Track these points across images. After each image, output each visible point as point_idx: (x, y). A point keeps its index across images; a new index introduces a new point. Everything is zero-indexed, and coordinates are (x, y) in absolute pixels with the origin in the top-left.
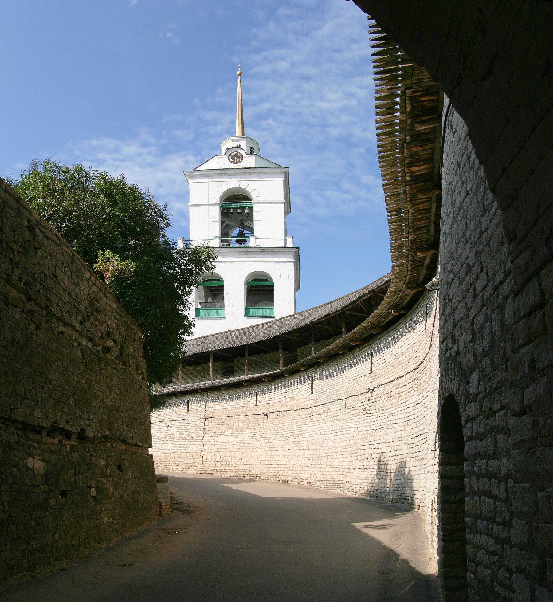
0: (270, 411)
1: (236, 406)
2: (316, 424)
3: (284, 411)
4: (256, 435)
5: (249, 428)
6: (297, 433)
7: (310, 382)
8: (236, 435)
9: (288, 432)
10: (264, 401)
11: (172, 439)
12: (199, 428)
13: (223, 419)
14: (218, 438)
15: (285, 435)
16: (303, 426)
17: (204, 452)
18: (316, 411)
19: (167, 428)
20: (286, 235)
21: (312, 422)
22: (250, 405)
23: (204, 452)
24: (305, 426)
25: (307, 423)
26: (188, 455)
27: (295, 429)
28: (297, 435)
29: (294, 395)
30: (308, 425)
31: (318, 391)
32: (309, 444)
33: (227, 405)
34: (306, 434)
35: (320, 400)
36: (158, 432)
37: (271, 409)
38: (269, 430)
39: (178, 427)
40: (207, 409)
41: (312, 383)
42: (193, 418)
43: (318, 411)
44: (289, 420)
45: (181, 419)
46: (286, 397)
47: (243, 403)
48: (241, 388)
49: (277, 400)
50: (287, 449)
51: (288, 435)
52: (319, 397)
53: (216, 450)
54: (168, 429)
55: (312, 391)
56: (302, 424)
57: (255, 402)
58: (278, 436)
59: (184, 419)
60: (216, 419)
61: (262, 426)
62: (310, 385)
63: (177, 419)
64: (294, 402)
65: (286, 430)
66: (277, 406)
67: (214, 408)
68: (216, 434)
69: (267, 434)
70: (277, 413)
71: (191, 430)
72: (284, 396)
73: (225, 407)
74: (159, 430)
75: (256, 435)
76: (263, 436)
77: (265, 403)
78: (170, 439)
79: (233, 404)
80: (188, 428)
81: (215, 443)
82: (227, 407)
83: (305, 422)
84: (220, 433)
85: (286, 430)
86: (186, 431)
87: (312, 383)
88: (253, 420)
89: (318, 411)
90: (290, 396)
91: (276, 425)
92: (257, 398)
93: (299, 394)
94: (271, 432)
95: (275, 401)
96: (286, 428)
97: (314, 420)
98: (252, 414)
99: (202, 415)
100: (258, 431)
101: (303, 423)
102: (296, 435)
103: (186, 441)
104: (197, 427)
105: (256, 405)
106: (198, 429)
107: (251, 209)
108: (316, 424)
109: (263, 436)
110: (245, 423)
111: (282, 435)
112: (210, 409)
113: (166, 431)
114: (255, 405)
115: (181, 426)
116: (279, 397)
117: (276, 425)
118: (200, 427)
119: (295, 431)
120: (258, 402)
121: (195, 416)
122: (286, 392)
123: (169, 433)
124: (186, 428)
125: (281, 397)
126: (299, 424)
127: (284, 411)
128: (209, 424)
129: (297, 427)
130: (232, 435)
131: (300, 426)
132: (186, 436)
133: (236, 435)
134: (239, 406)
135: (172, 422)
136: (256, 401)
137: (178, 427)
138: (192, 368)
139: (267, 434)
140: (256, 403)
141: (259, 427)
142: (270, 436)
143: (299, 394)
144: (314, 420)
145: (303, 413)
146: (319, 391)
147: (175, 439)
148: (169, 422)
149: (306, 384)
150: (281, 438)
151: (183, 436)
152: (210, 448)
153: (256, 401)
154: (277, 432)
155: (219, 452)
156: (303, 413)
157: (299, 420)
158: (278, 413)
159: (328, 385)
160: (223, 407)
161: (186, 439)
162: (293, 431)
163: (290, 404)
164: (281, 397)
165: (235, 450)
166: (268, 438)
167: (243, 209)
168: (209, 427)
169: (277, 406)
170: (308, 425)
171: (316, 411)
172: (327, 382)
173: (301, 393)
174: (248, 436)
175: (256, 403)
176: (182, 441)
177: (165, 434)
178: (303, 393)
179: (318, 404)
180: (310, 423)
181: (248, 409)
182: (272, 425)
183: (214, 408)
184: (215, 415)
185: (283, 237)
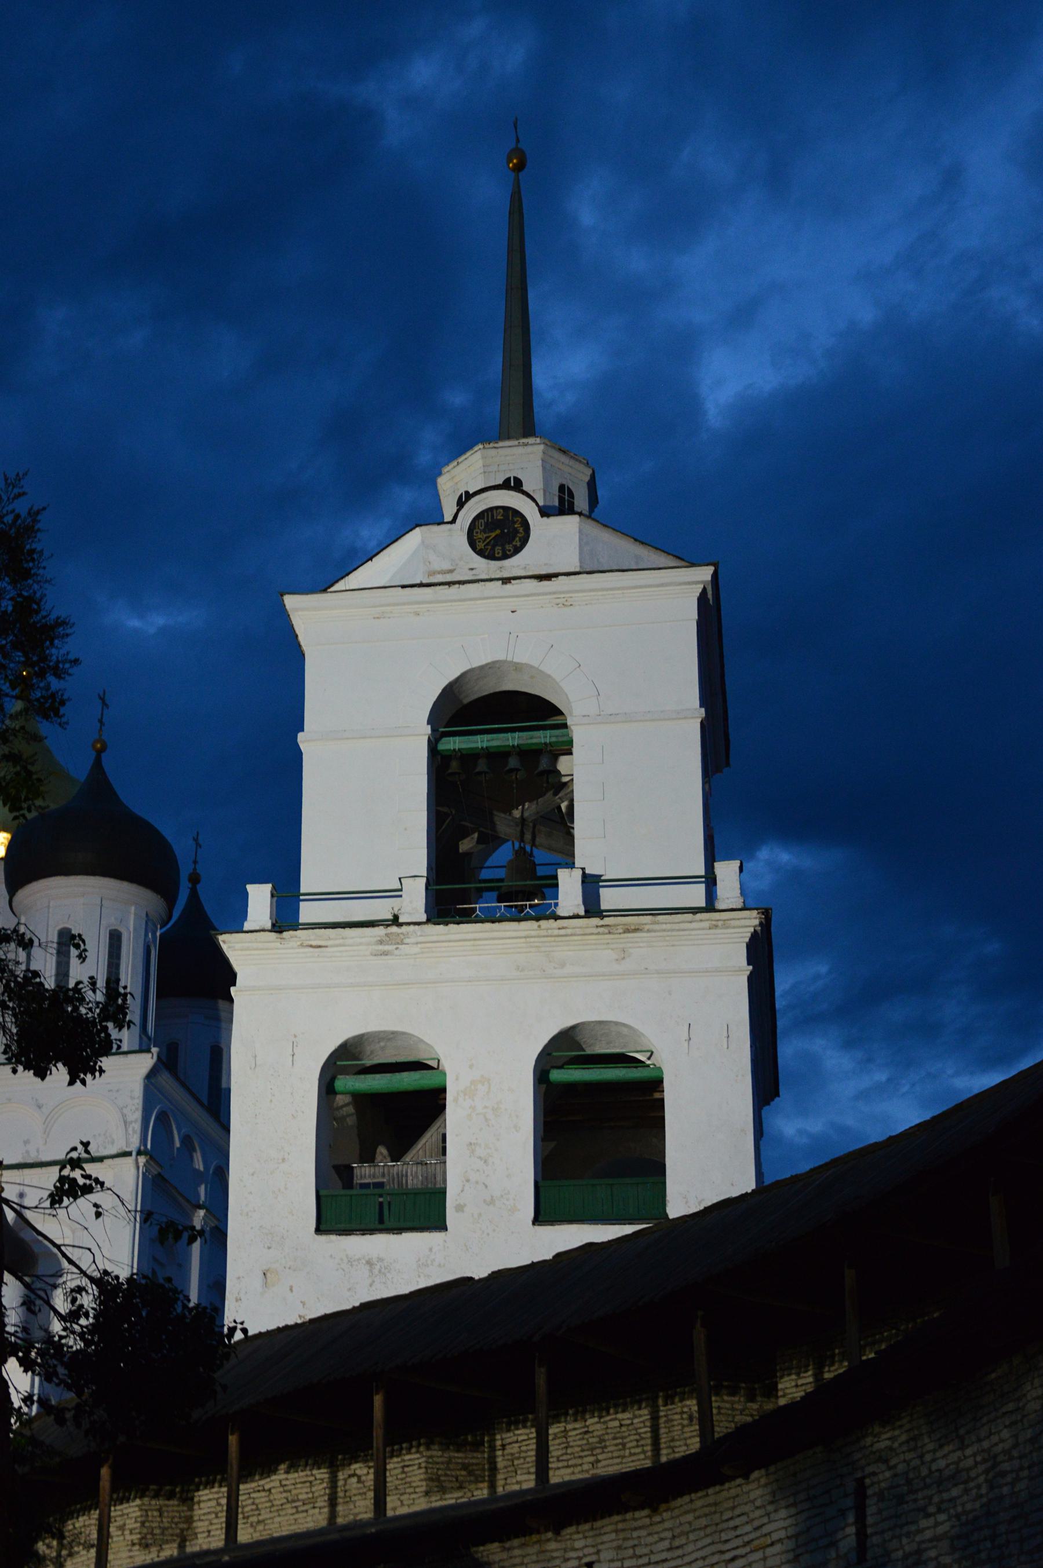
7: (850, 1502)
48: (516, 1542)
122: (728, 1556)
159: (940, 1510)
172: (936, 1499)
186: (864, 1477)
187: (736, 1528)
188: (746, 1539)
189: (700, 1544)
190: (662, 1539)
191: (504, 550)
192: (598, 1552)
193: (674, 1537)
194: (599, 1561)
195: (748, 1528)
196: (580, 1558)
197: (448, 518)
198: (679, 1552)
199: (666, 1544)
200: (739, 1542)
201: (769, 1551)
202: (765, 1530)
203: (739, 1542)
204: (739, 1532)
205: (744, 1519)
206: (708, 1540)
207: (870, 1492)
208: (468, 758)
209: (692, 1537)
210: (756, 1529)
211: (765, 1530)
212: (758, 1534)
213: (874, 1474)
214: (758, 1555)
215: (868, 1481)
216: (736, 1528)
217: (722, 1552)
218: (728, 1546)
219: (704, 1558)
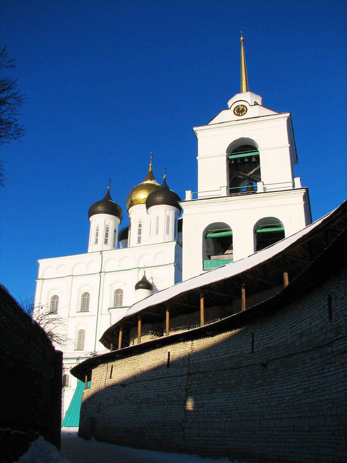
0: (271, 358)
1: (227, 356)
2: (341, 370)
3: (290, 355)
4: (254, 396)
5: (243, 385)
6: (311, 389)
7: (327, 302)
8: (226, 396)
9: (298, 388)
10: (262, 344)
11: (149, 405)
12: (180, 389)
13: (210, 376)
14: (205, 402)
15: (293, 394)
16: (319, 376)
17: (186, 421)
18: (339, 347)
19: (144, 390)
20: (293, 177)
21: (334, 368)
22: (245, 352)
23: (186, 421)
24: (323, 375)
25: (325, 371)
26: (166, 427)
27: (308, 383)
28: (312, 393)
29: (303, 329)
30: (328, 374)
31: (339, 314)
32: (330, 405)
33: (215, 355)
34: (326, 389)
35: (344, 328)
36: (134, 395)
37: (273, 355)
38: (271, 387)
39: (156, 388)
40: (191, 362)
41: (330, 304)
42: (174, 375)
43: (342, 347)
44: (298, 368)
45: (160, 377)
46: (293, 334)
47: (235, 350)
49: (281, 341)
50: (296, 415)
51: (297, 393)
52: (342, 323)
53: (201, 420)
54: (144, 392)
55: (330, 317)
56: (318, 372)
57: (250, 348)
58: (283, 395)
59: (163, 376)
60: (202, 376)
61: (260, 382)
62: (327, 307)
63: (155, 377)
64: (304, 339)
65: (295, 385)
66: (281, 349)
67: (199, 361)
68: (202, 396)
69: (268, 393)
70: (281, 360)
71: (170, 392)
72: (289, 334)
73: (213, 359)
74: (135, 392)
75: (254, 396)
76: (262, 397)
77: (265, 347)
78: (146, 405)
79: (223, 353)
80: (168, 389)
81: (200, 409)
82: (216, 358)
83: (323, 369)
84: (206, 395)
85: (295, 385)
86: (164, 393)
87: (330, 304)
88: (248, 374)
89: (342, 347)
90: (298, 332)
91: (280, 379)
92: (253, 342)
93: (311, 326)
94: (274, 389)
95: (277, 343)
96: (295, 381)
97: (337, 364)
98: (248, 364)
99: (185, 372)
100: (256, 389)
101: (319, 371)
102: (309, 391)
103: (165, 407)
104: (178, 388)
105: (253, 352)
106: (179, 390)
107: (258, 157)
108: (341, 370)
109: (262, 397)
110: (238, 379)
111: (289, 394)
112: (195, 362)
113: (142, 395)
114: (251, 351)
115: (160, 387)
116: (282, 336)
117: (280, 379)
118: (181, 388)
119: (308, 386)
120: (255, 347)
121: (176, 372)
122: (291, 326)
123: (146, 397)
124: (163, 390)
125: (285, 335)
126: (314, 373)
127: (290, 355)
128: (194, 382)
129: (311, 378)
130: (222, 396)
131: (315, 377)
132: (165, 400)
133: (226, 396)
134: (230, 355)
135: (149, 382)
136: (253, 345)
137: (156, 388)
138: (185, 317)
139: (268, 393)
140: (253, 349)
141: (256, 383)
142: (272, 396)
143: (311, 326)
144: (337, 364)
145: (318, 355)
146: (341, 313)
147: (152, 404)
148: (146, 382)
149: (320, 307)
150: (287, 398)
151: (161, 399)
152: (193, 417)
153: (253, 345)
154: (281, 388)
155: (204, 422)
156: (318, 355)
157: (312, 367)
158: (283, 359)
160: (210, 359)
161: (164, 405)
162: (305, 386)
163: (298, 343)
164: (285, 335)
165: (225, 419)
166: (269, 400)
167: (250, 158)
168: (192, 386)
169: (281, 349)
170: (328, 374)
171: (339, 347)
173: (313, 324)
174: (242, 397)
175: (253, 349)
176: (160, 407)
177: (141, 398)
178: (317, 322)
179: (341, 336)
180: (331, 369)
181: (242, 358)
182: (273, 379)
183: (199, 361)
184: (200, 370)
185: (290, 179)
186: (330, 294)
187: (293, 317)
188: (296, 320)
189: (283, 324)
190: (272, 324)
191: (242, 114)
192: (255, 330)
193: (276, 323)
194: (255, 332)
195: (296, 317)
196: (250, 332)
197: (229, 108)
198: (277, 327)
199: (273, 325)
200: (294, 321)
201: (302, 323)
202: (301, 317)
203: (294, 321)
204: (294, 318)
205: (295, 314)
206: (285, 322)
207: (332, 299)
208: (236, 160)
209: (281, 322)
210: (299, 317)
211: (301, 317)
212: (299, 318)
213: (334, 292)
214: (300, 324)
215: (332, 295)
216: (293, 317)
217: (289, 325)
218: (290, 323)
219: (284, 328)
